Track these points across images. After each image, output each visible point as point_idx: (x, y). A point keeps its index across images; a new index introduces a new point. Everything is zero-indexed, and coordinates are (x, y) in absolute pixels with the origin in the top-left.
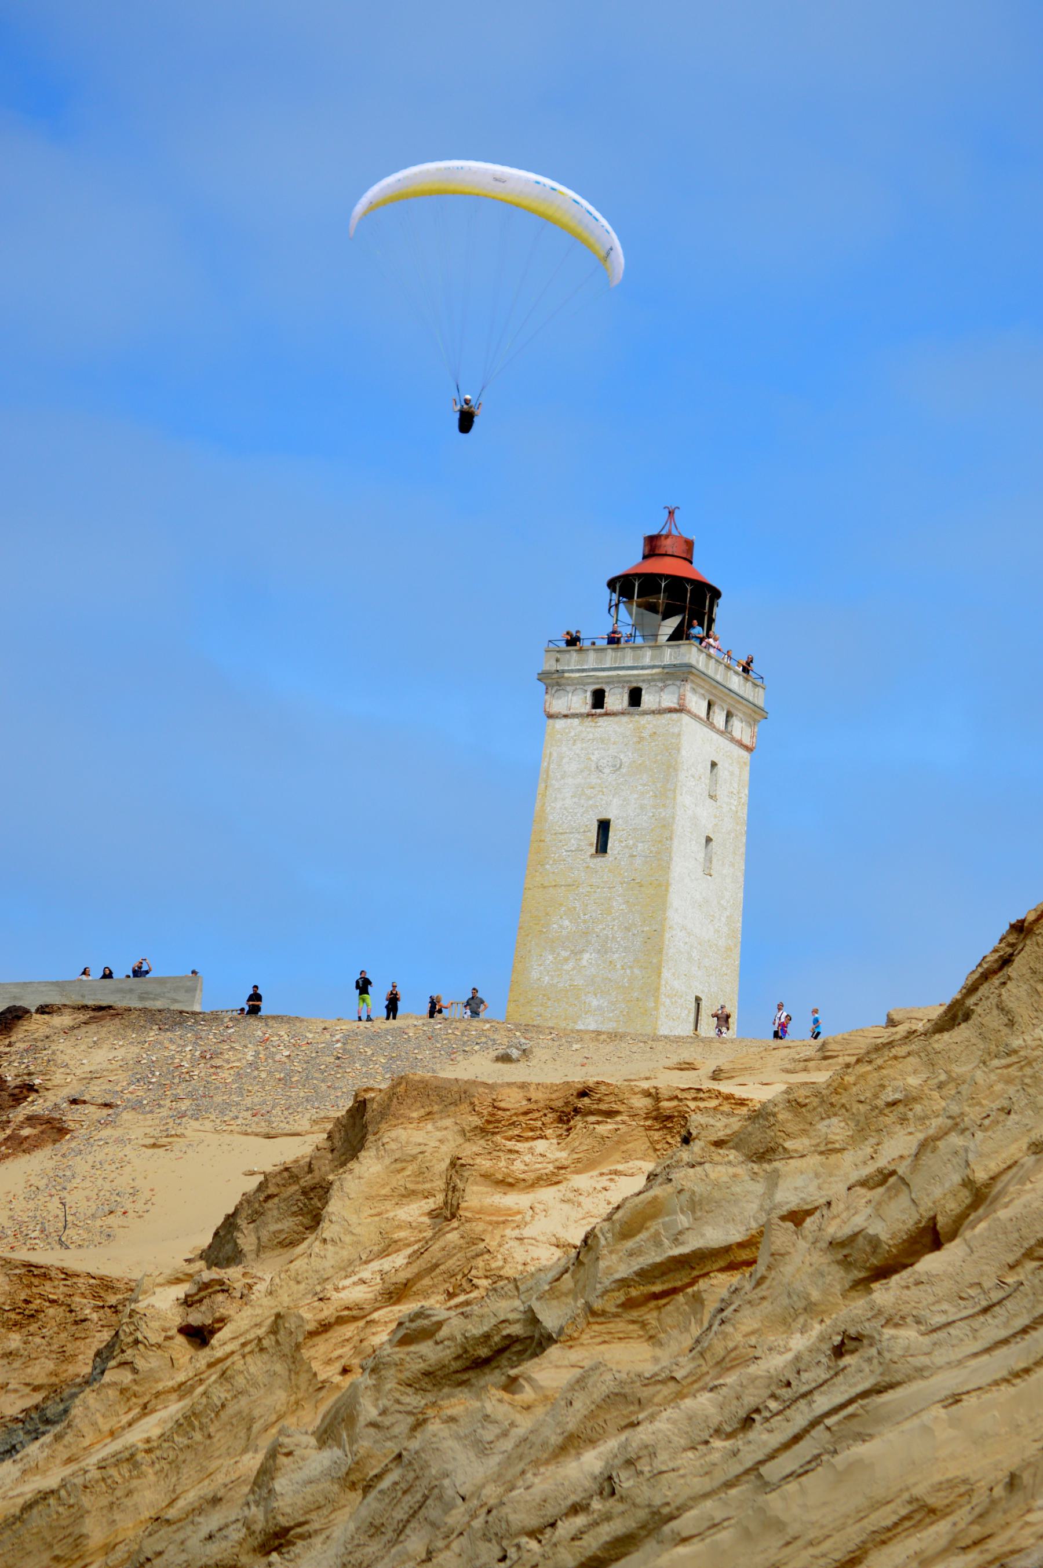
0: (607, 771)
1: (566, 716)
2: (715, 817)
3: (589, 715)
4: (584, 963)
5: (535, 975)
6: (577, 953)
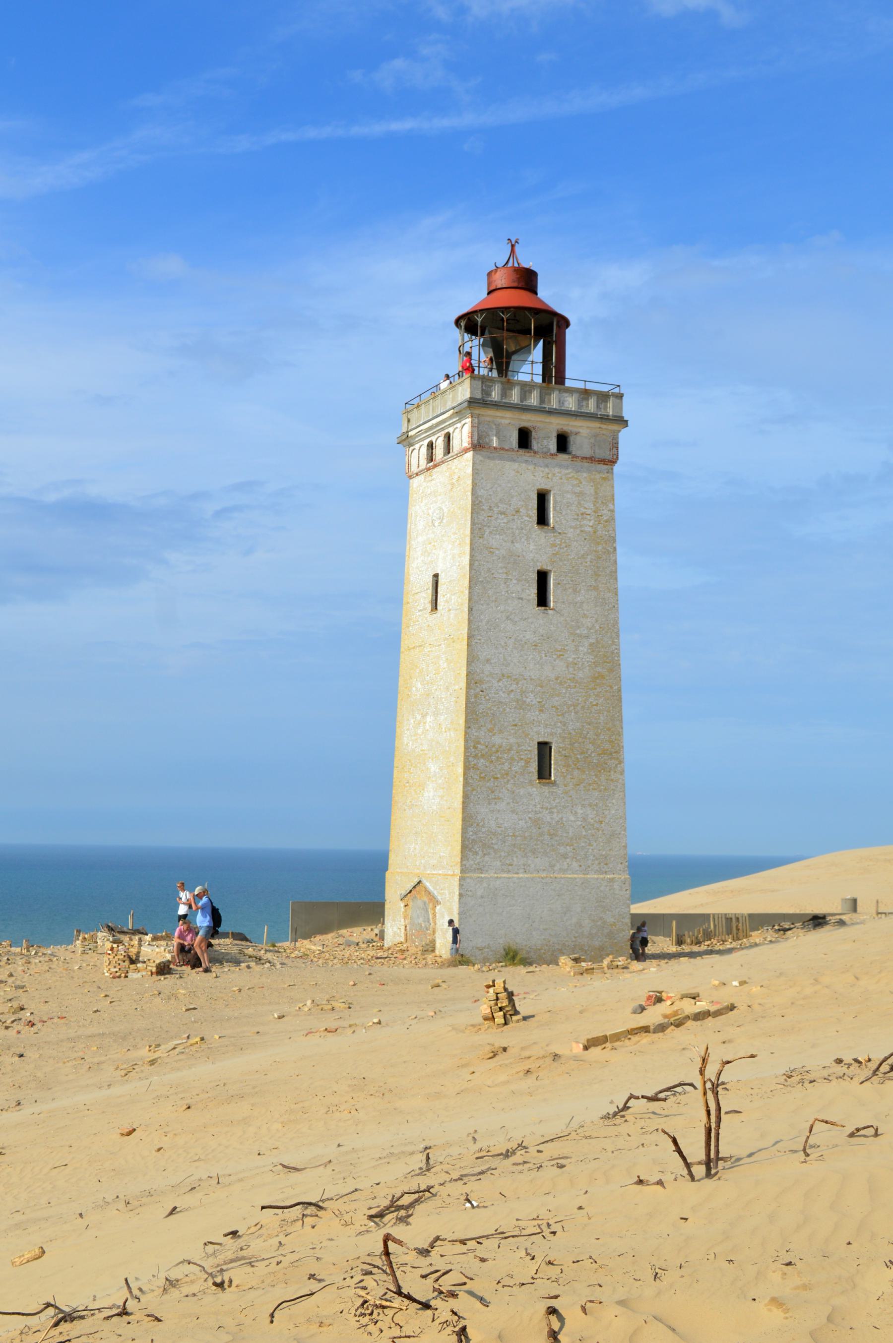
0: (436, 524)
1: (417, 474)
2: (553, 545)
3: (428, 469)
4: (428, 727)
5: (405, 740)
6: (424, 716)
